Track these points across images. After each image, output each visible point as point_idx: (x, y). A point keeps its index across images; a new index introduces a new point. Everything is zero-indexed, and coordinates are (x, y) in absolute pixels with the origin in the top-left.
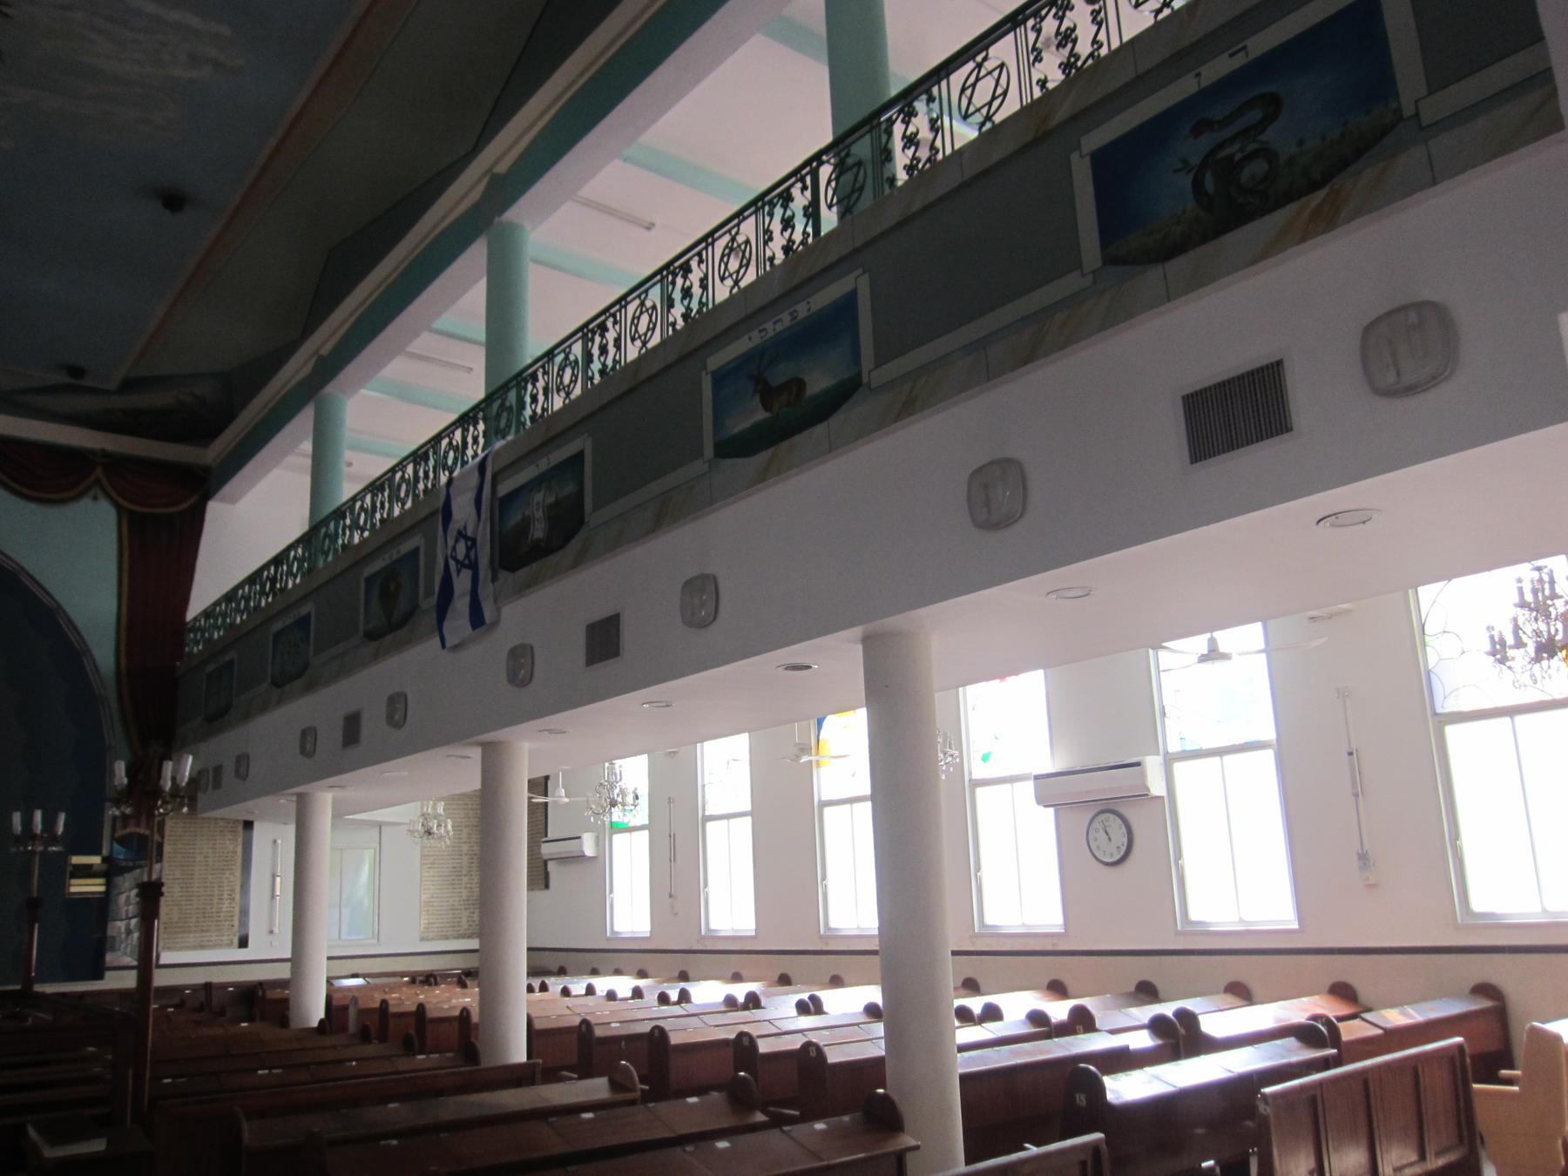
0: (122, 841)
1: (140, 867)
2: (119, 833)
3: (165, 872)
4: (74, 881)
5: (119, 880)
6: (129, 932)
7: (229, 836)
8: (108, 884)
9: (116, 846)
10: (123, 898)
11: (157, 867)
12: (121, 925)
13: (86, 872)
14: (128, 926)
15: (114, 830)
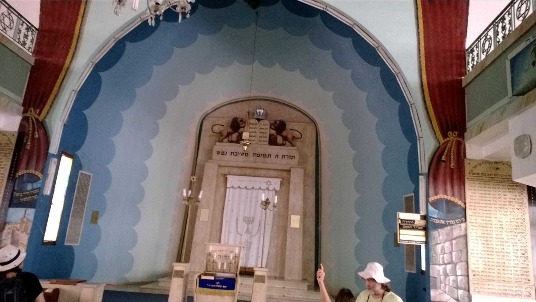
0: (435, 204)
1: (450, 225)
2: (431, 199)
3: (470, 230)
4: (402, 231)
5: (435, 233)
6: (446, 275)
7: (516, 206)
8: (427, 236)
9: (431, 208)
10: (439, 247)
11: (463, 225)
12: (441, 268)
13: (411, 225)
14: (445, 269)
15: (428, 196)
